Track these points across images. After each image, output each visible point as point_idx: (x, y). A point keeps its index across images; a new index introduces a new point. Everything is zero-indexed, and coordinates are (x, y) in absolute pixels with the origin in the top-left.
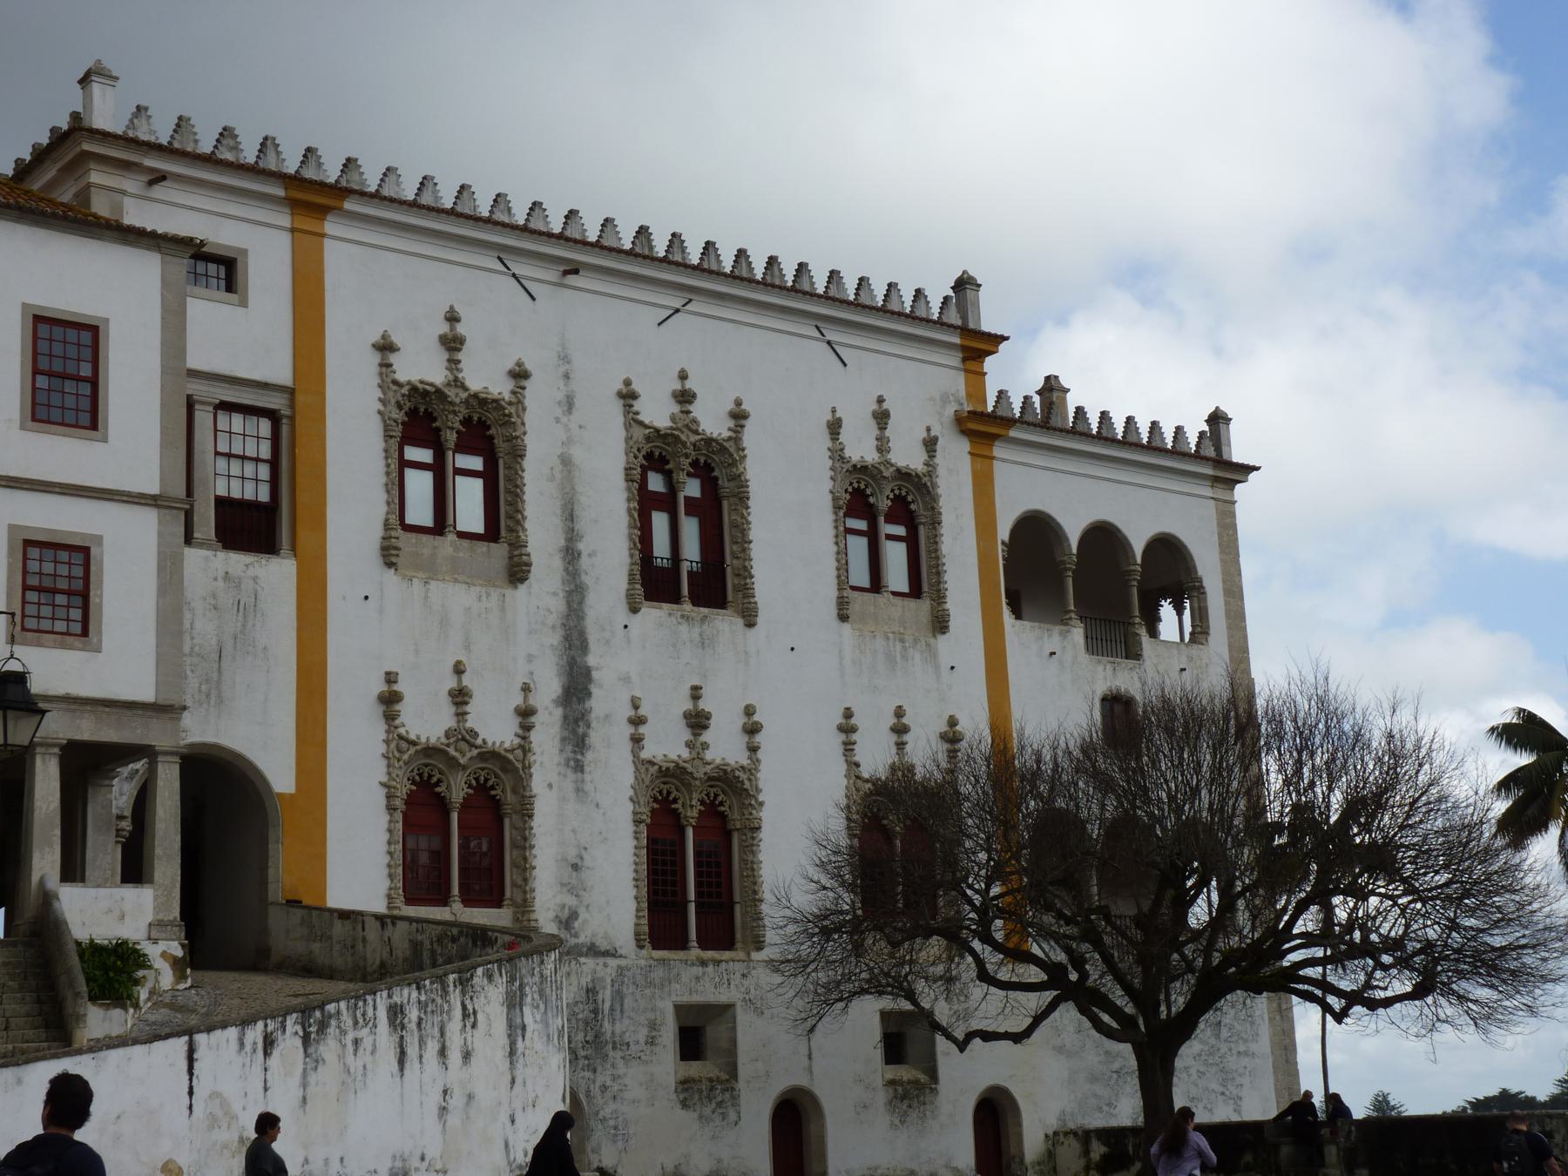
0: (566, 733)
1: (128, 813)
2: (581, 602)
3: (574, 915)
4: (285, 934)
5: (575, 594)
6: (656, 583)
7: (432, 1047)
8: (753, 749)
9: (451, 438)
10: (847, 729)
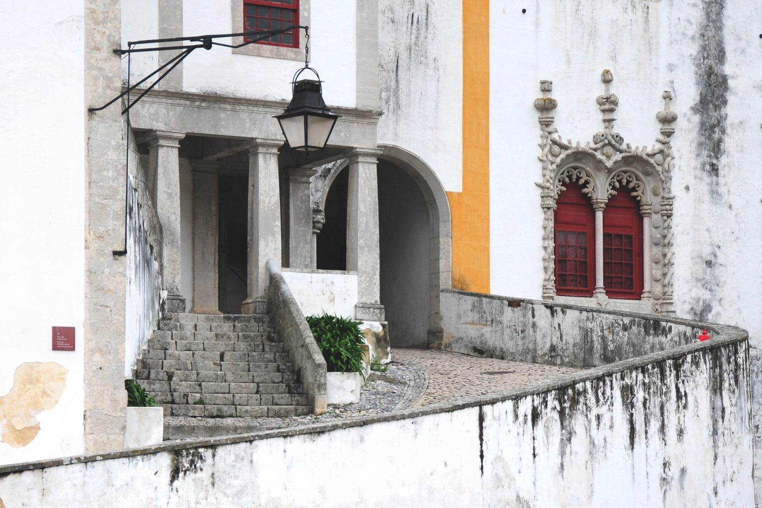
0: (703, 139)
1: (322, 208)
2: (719, 14)
3: (707, 308)
4: (455, 316)
7: (655, 425)
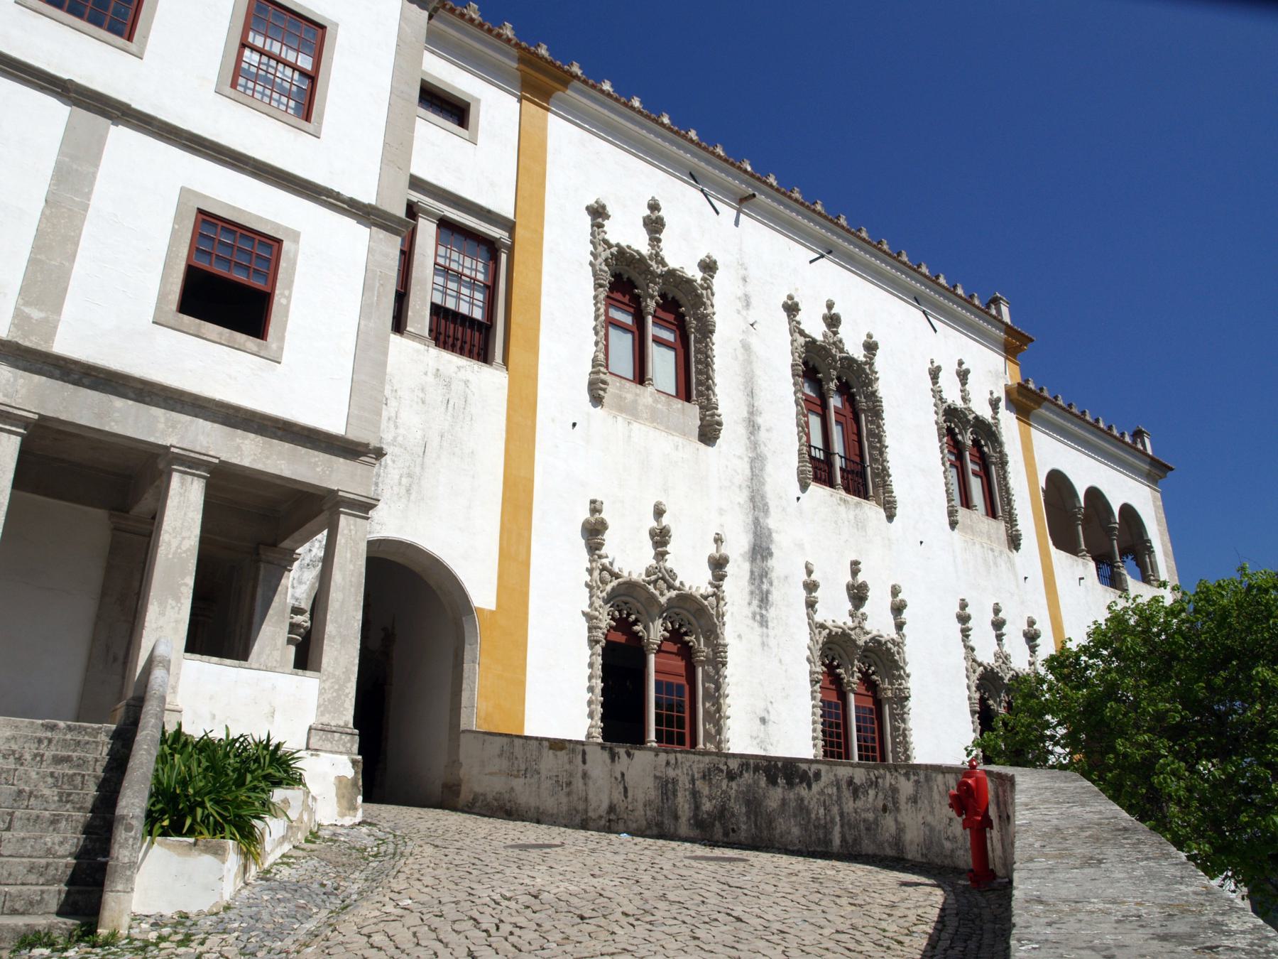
1: (306, 605)
5: (757, 462)
6: (819, 470)
8: (900, 626)
9: (651, 305)
10: (963, 619)
